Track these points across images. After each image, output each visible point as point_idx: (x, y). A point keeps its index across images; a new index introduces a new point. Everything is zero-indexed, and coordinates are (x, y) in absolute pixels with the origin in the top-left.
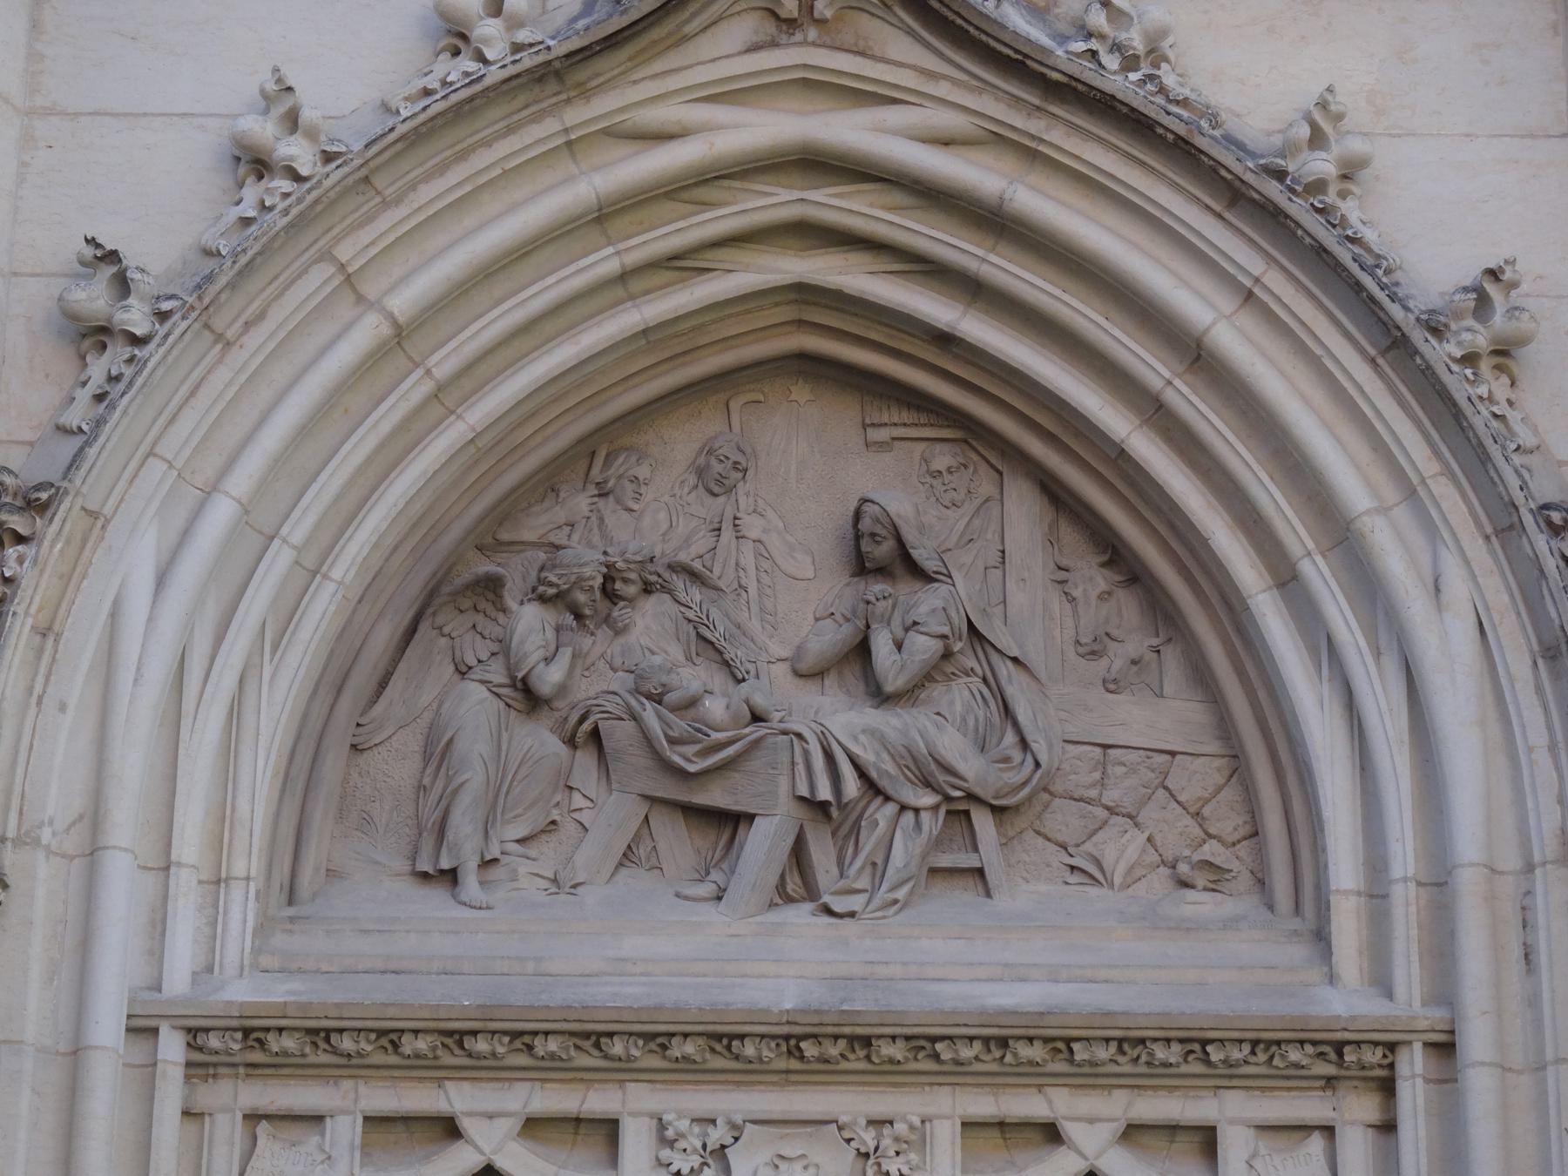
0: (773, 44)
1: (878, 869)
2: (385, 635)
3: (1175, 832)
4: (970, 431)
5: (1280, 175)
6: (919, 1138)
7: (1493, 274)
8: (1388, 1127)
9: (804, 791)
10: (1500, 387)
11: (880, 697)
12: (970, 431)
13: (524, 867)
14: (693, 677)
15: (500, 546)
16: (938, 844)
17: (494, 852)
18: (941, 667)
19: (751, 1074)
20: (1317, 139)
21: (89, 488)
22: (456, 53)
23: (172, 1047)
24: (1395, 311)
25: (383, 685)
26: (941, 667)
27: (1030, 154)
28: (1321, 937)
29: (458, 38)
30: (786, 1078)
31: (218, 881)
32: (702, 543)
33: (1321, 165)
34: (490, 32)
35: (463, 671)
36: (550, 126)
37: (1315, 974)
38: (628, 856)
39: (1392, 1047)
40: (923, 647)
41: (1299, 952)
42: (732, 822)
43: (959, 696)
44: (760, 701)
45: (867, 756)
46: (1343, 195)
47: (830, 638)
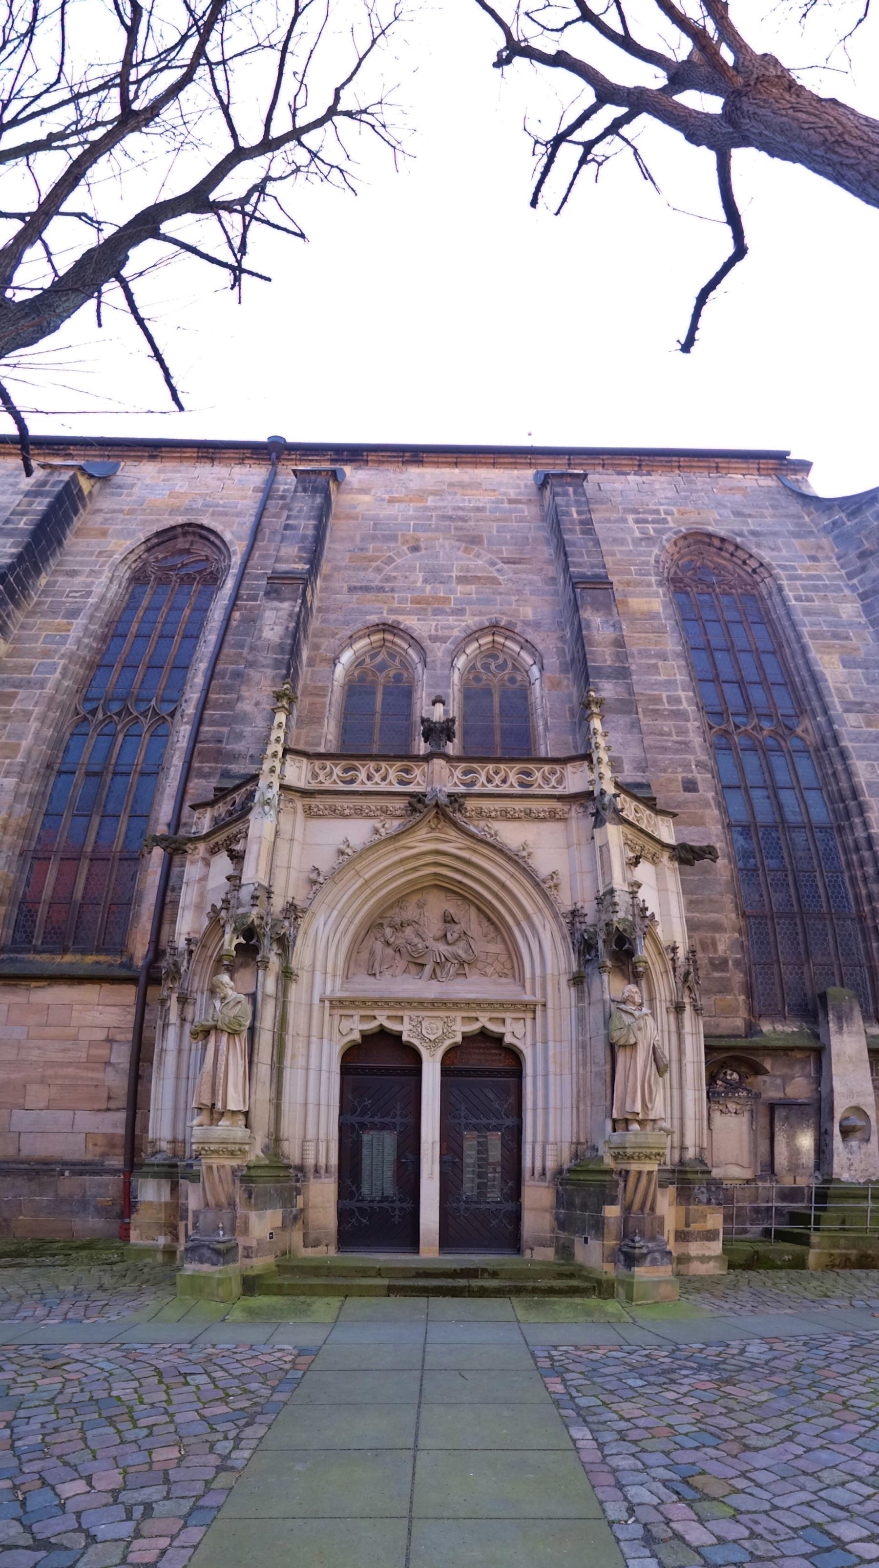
1: (448, 974)
2: (363, 933)
3: (498, 967)
4: (465, 898)
6: (454, 1020)
8: (534, 1019)
11: (448, 944)
12: (465, 898)
14: (416, 940)
18: (459, 939)
19: (426, 1009)
20: (524, 849)
21: (313, 908)
23: (327, 1004)
26: (459, 939)
27: (475, 851)
28: (524, 986)
29: (376, 831)
30: (432, 1010)
31: (334, 976)
33: (525, 854)
34: (382, 830)
40: (456, 935)
41: (520, 988)
42: (423, 965)
43: (462, 944)
47: (441, 933)
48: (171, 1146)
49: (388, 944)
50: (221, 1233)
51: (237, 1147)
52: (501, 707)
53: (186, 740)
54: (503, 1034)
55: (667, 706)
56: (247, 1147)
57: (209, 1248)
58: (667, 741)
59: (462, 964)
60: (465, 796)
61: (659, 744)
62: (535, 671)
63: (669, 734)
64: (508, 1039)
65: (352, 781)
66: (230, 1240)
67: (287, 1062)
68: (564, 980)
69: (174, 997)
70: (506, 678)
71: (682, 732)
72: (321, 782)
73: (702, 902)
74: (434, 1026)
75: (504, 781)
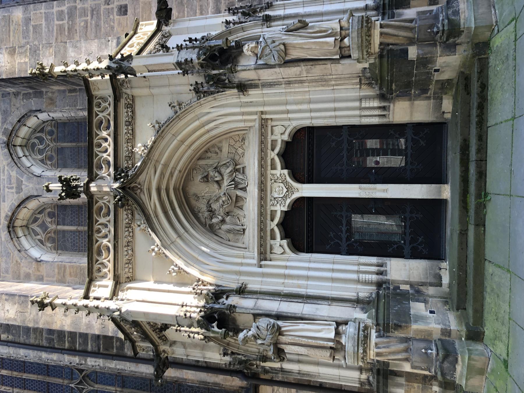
0: (144, 192)
1: (243, 180)
3: (238, 144)
5: (158, 131)
6: (273, 175)
7: (170, 105)
8: (271, 119)
9: (233, 188)
10: (183, 104)
11: (223, 179)
13: (243, 221)
15: (206, 225)
16: (239, 172)
17: (241, 224)
19: (266, 195)
22: (145, 230)
23: (263, 263)
24: (174, 117)
25: (222, 238)
27: (158, 161)
28: (250, 127)
30: (266, 191)
32: (205, 200)
33: (157, 126)
35: (220, 228)
36: (154, 219)
37: (254, 128)
38: (242, 209)
39: (262, 119)
40: (217, 174)
42: (237, 196)
43: (223, 170)
44: (223, 193)
45: (229, 181)
46: (161, 123)
47: (216, 186)
48: (364, 372)
49: (223, 221)
50: (429, 351)
51: (361, 333)
52: (71, 142)
53: (97, 360)
54: (282, 140)
55: (65, 22)
56: (362, 325)
57: (442, 362)
58: (91, 24)
59: (236, 170)
60: (116, 168)
61: (94, 30)
62: (43, 116)
63: (86, 22)
64: (286, 137)
65: (108, 249)
66: (436, 345)
67: (302, 291)
68: (244, 99)
69: (262, 364)
70: (50, 138)
71: (84, 12)
72: (109, 271)
73: (201, 6)
74: (277, 189)
75: (106, 140)
